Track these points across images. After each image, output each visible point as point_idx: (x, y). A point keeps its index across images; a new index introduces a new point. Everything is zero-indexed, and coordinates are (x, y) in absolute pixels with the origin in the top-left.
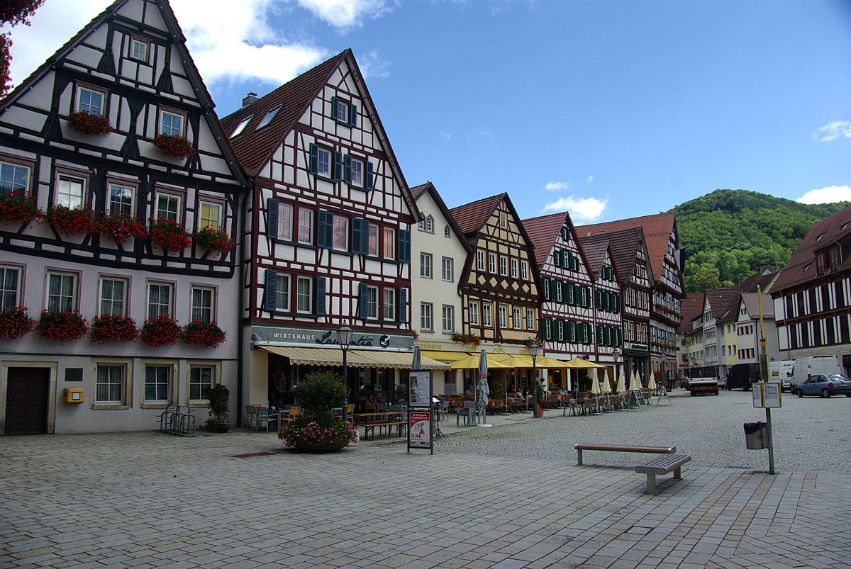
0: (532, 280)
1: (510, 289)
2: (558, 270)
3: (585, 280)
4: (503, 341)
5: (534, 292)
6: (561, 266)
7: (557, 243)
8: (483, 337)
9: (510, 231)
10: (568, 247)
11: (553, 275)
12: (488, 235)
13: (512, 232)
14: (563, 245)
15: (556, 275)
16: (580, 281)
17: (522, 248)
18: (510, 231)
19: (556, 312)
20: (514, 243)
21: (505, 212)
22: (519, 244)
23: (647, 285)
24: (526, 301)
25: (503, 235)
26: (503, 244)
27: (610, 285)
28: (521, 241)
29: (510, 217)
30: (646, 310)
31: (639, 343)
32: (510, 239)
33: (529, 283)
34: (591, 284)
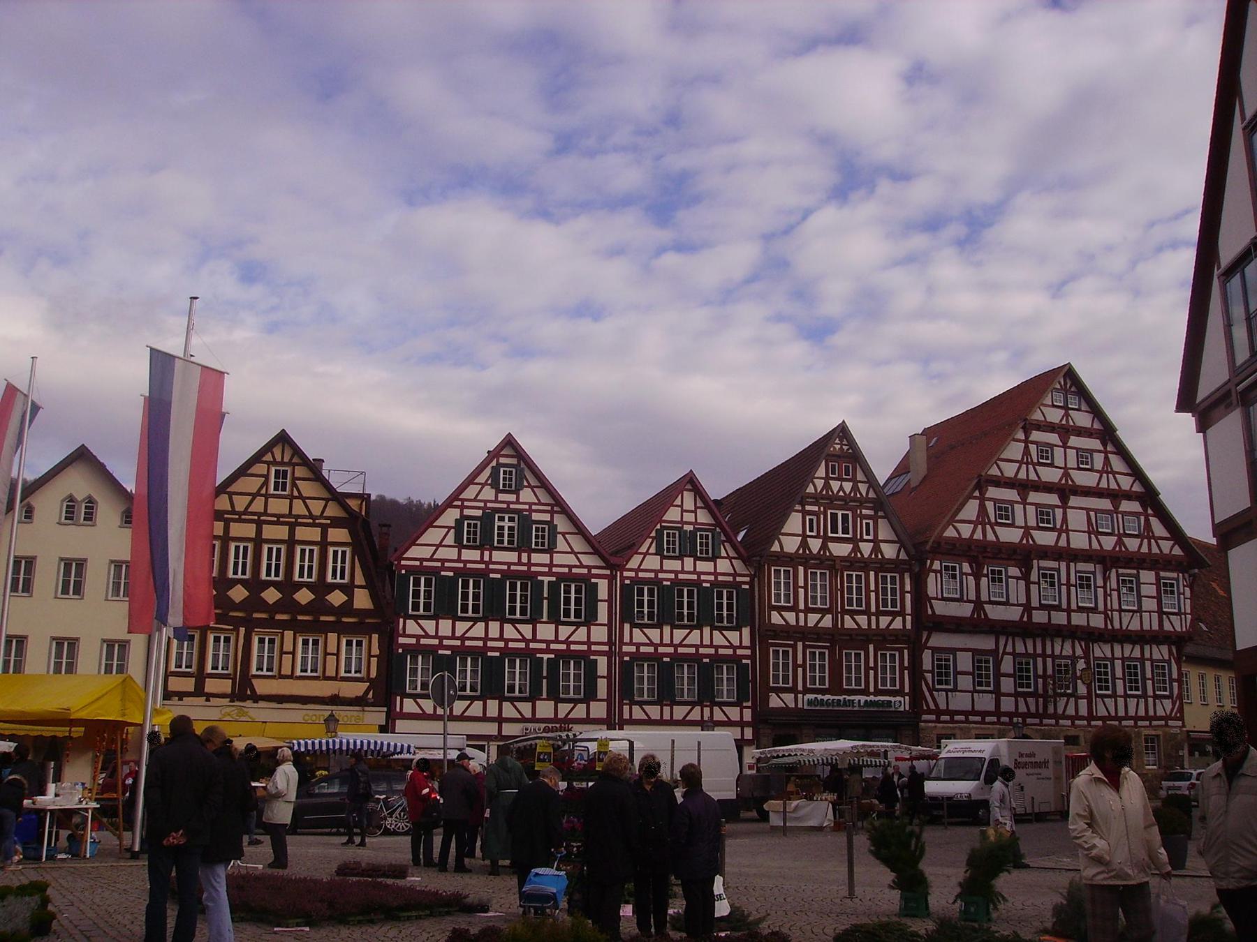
0: (359, 579)
1: (287, 604)
2: (471, 555)
3: (581, 566)
4: (256, 698)
5: (362, 600)
6: (485, 544)
7: (475, 500)
8: (199, 691)
9: (300, 497)
10: (518, 502)
11: (447, 564)
12: (233, 512)
13: (304, 499)
14: (496, 501)
15: (461, 565)
16: (554, 570)
17: (336, 523)
18: (300, 497)
19: (453, 637)
20: (311, 516)
21: (290, 464)
22: (327, 518)
23: (889, 551)
24: (338, 622)
25: (279, 506)
26: (277, 523)
27: (704, 566)
28: (333, 510)
29: (300, 472)
30: (902, 613)
31: (865, 692)
32: (299, 508)
33: (348, 589)
34: (608, 572)
